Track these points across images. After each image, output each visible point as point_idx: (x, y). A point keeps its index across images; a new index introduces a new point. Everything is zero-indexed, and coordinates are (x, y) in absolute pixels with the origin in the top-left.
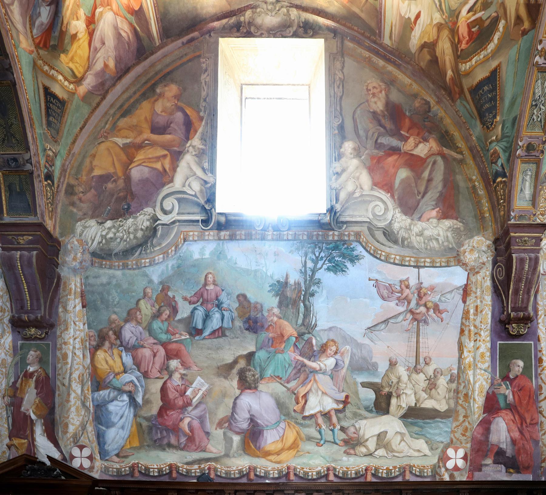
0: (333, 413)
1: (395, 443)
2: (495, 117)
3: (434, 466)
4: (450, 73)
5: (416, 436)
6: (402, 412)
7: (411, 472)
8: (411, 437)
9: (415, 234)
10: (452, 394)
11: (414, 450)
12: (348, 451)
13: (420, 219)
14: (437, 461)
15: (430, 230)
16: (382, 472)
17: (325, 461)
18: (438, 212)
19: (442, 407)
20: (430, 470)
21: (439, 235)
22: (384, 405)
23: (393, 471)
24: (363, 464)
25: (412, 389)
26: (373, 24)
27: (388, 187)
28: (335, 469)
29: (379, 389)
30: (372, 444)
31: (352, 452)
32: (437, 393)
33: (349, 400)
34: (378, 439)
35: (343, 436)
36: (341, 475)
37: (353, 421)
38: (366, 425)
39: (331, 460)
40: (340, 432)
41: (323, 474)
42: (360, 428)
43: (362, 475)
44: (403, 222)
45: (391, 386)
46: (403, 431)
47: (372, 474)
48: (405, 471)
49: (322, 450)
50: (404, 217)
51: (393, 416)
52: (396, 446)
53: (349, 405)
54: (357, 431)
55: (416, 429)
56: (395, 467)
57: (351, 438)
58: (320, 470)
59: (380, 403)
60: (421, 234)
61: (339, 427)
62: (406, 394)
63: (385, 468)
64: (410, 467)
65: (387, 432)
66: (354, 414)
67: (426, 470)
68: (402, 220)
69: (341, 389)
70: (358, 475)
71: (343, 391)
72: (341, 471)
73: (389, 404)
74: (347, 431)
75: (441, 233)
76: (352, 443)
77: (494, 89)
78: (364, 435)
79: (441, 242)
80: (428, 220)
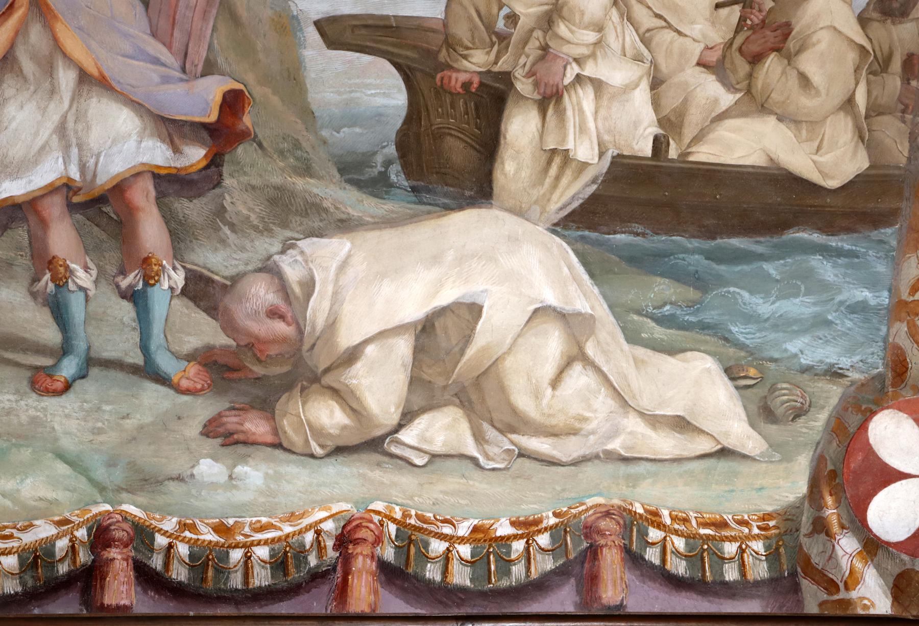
0: (143, 196)
1: (531, 371)
3: (788, 518)
5: (659, 332)
6: (572, 191)
7: (634, 559)
8: (633, 337)
10: (894, 82)
11: (654, 421)
12: (231, 421)
14: (802, 488)
16: (447, 557)
17: (82, 483)
19: (832, 159)
20: (758, 546)
22: (458, 151)
23: (518, 546)
24: (323, 504)
25: (638, 58)
28: (142, 534)
29: (430, 54)
30: (380, 384)
31: (256, 426)
32: (793, 81)
33: (247, 120)
34: (419, 350)
35: (202, 331)
36: (180, 574)
37: (267, 245)
38: (343, 266)
39: (118, 476)
40: (182, 307)
41: (63, 569)
42: (309, 286)
43: (318, 577)
45: (503, 38)
46: (581, 305)
47: (384, 567)
48: (593, 553)
49: (64, 416)
51: (518, 212)
52: (537, 395)
53: (243, 151)
54: (291, 301)
55: (662, 290)
56: (528, 527)
57: (252, 346)
58: (50, 542)
59: (438, 136)
61: (179, 279)
62: (598, 85)
63: (463, 530)
64: (627, 528)
65: (474, 310)
66: (273, 202)
67: (730, 549)
69: (199, 55)
70: (294, 575)
71: (210, 68)
72: (183, 550)
73: (489, 145)
74: (228, 301)
76: (259, 378)
78: (332, 325)
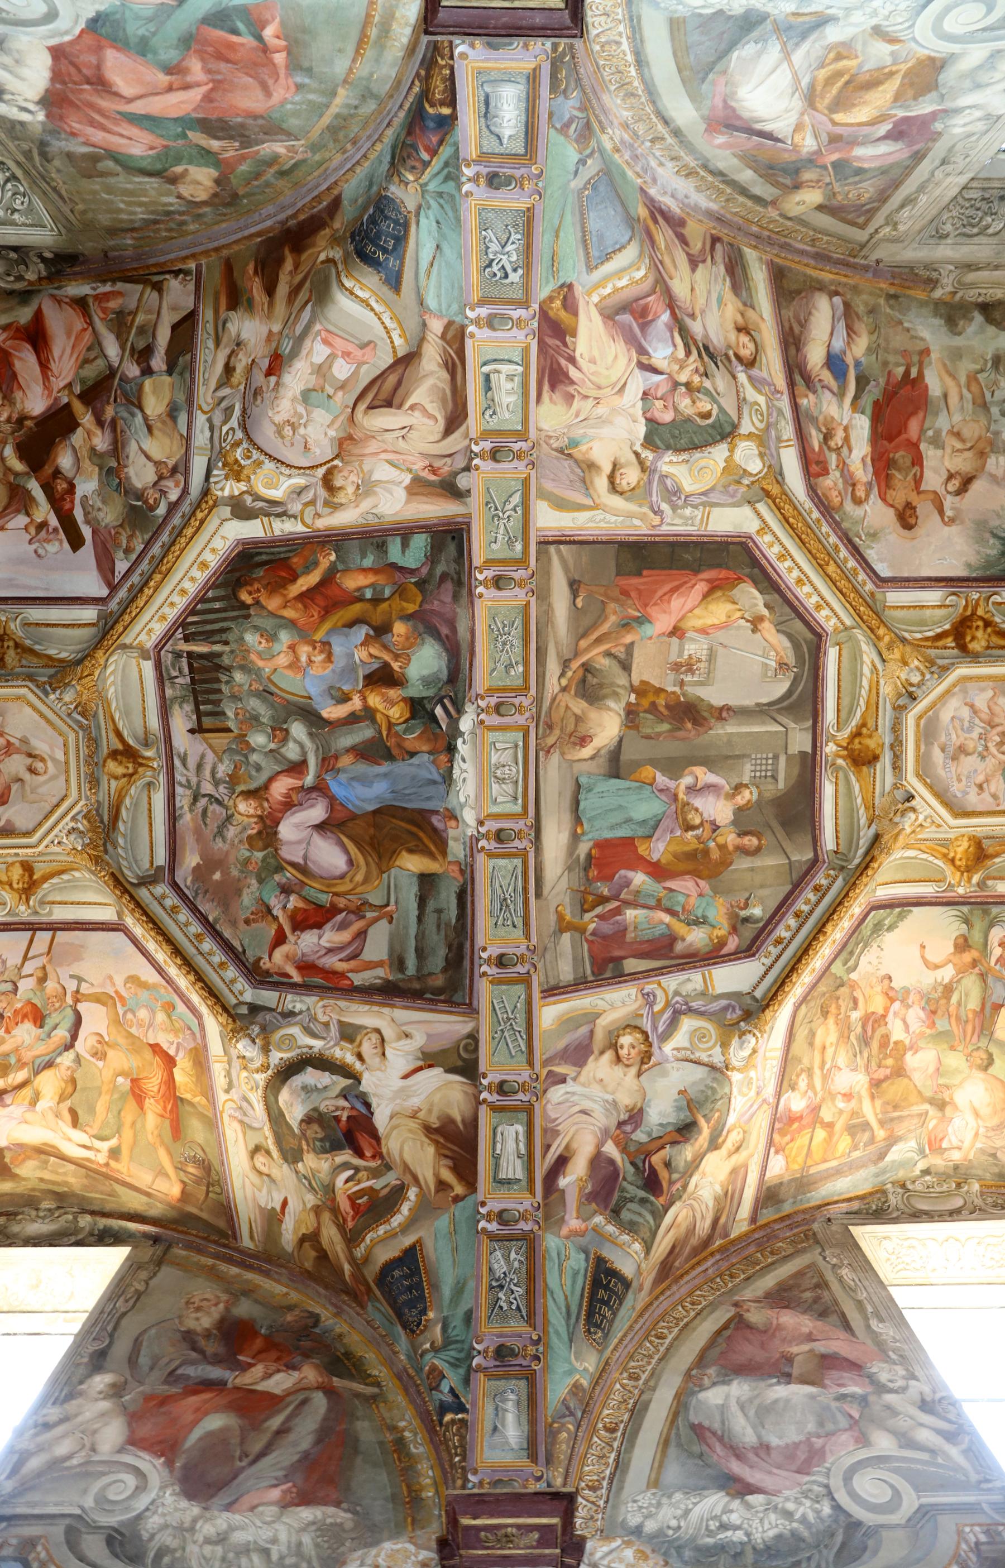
2: (424, 1312)
4: (347, 1267)
9: (201, 1539)
13: (228, 1507)
15: (252, 1530)
18: (284, 1492)
21: (274, 1541)
26: (221, 1224)
27: (165, 1448)
44: (178, 1514)
50: (184, 1503)
60: (221, 1539)
68: (176, 1509)
75: (283, 1537)
77: (415, 1271)
79: (275, 1557)
80: (252, 1509)
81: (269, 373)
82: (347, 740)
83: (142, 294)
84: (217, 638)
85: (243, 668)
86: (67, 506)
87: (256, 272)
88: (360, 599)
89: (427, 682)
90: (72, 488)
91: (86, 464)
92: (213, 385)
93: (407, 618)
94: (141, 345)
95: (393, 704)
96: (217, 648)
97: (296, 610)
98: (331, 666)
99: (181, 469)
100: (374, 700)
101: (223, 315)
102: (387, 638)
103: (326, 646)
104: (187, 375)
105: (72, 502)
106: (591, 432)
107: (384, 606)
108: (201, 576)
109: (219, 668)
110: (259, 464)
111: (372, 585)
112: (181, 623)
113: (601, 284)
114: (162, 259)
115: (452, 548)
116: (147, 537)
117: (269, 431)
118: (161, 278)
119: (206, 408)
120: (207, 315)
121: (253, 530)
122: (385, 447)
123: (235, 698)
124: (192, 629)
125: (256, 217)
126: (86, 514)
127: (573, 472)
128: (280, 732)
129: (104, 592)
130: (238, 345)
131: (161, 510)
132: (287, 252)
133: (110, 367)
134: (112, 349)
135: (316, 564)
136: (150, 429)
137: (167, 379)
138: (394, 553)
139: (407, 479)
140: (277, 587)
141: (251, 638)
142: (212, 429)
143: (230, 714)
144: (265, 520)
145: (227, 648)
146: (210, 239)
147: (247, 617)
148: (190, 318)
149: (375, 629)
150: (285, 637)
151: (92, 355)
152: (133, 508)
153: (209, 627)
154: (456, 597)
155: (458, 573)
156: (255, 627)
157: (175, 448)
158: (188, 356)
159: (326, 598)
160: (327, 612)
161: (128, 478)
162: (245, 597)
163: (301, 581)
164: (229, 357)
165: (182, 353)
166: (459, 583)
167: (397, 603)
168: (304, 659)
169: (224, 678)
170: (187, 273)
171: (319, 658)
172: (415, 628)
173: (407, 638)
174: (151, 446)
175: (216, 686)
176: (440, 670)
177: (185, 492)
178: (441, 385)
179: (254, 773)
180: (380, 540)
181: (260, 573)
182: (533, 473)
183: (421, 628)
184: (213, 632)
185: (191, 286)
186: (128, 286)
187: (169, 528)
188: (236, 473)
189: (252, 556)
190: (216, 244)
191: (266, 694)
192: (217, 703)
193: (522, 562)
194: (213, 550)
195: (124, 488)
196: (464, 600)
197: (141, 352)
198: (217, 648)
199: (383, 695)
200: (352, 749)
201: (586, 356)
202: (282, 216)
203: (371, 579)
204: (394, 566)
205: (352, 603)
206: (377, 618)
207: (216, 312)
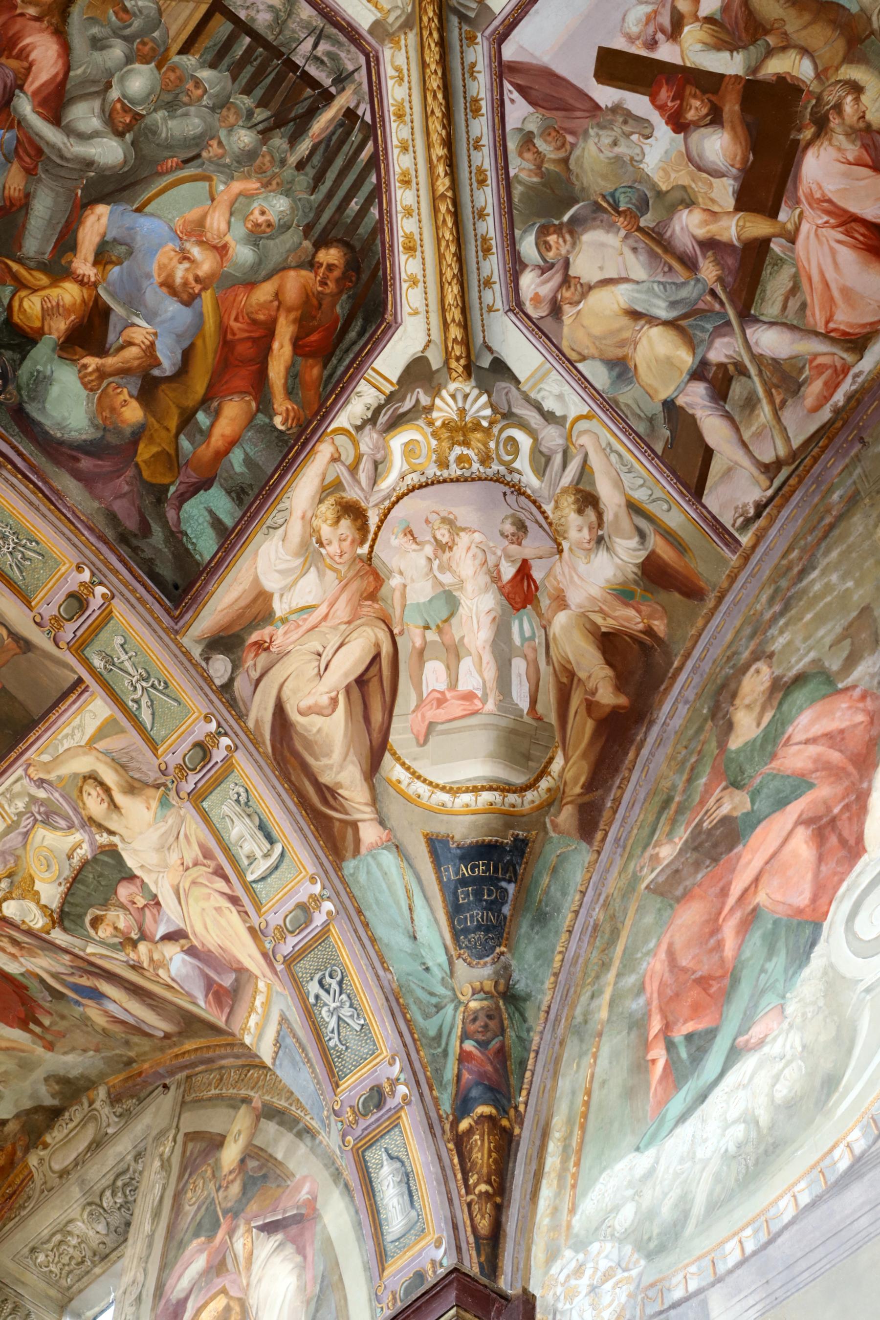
81: (524, 571)
82: (44, 207)
83: (787, 440)
84: (316, 160)
85: (248, 157)
86: (664, 94)
87: (649, 631)
88: (205, 402)
89: (42, 382)
90: (679, 124)
91: (683, 177)
92: (596, 462)
93: (139, 434)
94: (737, 390)
95: (46, 313)
96: (304, 147)
97: (262, 306)
98: (157, 279)
99: (545, 329)
100: (69, 293)
101: (655, 542)
102: (134, 384)
103: (188, 298)
104: (641, 428)
105: (661, 108)
106: (163, 828)
107: (173, 423)
108: (404, 227)
109: (278, 122)
110: (443, 463)
111: (207, 434)
112: (373, 130)
113: (267, 1004)
114: (785, 513)
115: (167, 572)
116: (518, 191)
117: (465, 515)
118: (777, 483)
119: (583, 425)
120: (676, 515)
121: (391, 360)
122: (330, 623)
123: (221, 104)
124: (355, 137)
125: (690, 694)
126: (629, 116)
127: (139, 770)
128: (124, 122)
129: (509, 52)
130: (600, 540)
131: (528, 246)
132: (622, 700)
133: (756, 320)
134: (771, 341)
135: (290, 393)
136: (635, 315)
137: (664, 395)
138: (218, 500)
139: (280, 608)
140: (308, 312)
141: (278, 206)
142: (549, 417)
143: (205, 74)
144: (388, 389)
145: (293, 160)
146: (735, 603)
147: (308, 230)
148: (696, 489)
149: (157, 382)
150: (243, 254)
151: (794, 304)
152: (574, 201)
153: (339, 162)
154: (112, 518)
155: (135, 550)
156: (285, 227)
157: (580, 334)
158: (659, 448)
159: (240, 359)
160: (226, 343)
161: (611, 227)
162: (331, 256)
163: (288, 350)
164: (600, 515)
165: (671, 444)
166: (124, 538)
167: (163, 441)
168: (196, 252)
169: (261, 114)
170: (748, 523)
171: (180, 273)
172: (118, 431)
173: (113, 410)
174: (620, 297)
175: (259, 92)
176: (43, 410)
177: (516, 306)
178: (325, 761)
179: (95, 30)
180: (248, 500)
181: (340, 310)
182: (156, 762)
183: (112, 439)
184: (328, 162)
185: (727, 519)
186: (812, 428)
187: (495, 243)
188: (459, 431)
189: (367, 322)
190: (729, 598)
191: (192, 153)
192: (235, 71)
193: (79, 647)
194: (415, 283)
195: (606, 209)
196: (101, 523)
197: (728, 380)
198: (304, 147)
199: (68, 311)
200: (25, 204)
201: (227, 912)
202: (655, 730)
203: (217, 440)
204: (205, 484)
205: (210, 387)
206: (167, 397)
207: (668, 535)
